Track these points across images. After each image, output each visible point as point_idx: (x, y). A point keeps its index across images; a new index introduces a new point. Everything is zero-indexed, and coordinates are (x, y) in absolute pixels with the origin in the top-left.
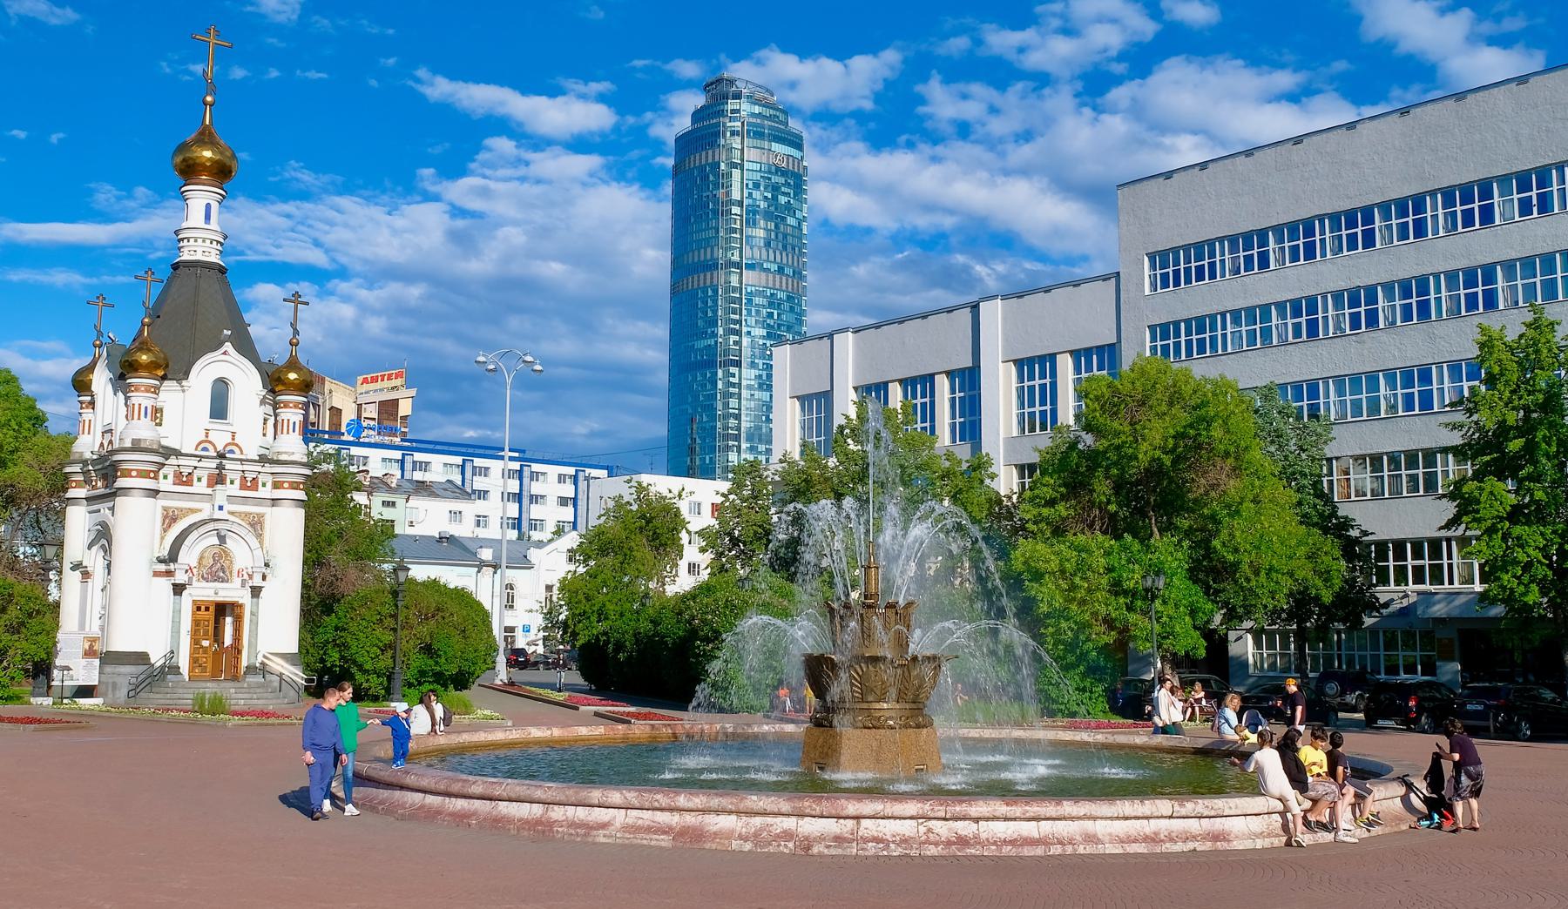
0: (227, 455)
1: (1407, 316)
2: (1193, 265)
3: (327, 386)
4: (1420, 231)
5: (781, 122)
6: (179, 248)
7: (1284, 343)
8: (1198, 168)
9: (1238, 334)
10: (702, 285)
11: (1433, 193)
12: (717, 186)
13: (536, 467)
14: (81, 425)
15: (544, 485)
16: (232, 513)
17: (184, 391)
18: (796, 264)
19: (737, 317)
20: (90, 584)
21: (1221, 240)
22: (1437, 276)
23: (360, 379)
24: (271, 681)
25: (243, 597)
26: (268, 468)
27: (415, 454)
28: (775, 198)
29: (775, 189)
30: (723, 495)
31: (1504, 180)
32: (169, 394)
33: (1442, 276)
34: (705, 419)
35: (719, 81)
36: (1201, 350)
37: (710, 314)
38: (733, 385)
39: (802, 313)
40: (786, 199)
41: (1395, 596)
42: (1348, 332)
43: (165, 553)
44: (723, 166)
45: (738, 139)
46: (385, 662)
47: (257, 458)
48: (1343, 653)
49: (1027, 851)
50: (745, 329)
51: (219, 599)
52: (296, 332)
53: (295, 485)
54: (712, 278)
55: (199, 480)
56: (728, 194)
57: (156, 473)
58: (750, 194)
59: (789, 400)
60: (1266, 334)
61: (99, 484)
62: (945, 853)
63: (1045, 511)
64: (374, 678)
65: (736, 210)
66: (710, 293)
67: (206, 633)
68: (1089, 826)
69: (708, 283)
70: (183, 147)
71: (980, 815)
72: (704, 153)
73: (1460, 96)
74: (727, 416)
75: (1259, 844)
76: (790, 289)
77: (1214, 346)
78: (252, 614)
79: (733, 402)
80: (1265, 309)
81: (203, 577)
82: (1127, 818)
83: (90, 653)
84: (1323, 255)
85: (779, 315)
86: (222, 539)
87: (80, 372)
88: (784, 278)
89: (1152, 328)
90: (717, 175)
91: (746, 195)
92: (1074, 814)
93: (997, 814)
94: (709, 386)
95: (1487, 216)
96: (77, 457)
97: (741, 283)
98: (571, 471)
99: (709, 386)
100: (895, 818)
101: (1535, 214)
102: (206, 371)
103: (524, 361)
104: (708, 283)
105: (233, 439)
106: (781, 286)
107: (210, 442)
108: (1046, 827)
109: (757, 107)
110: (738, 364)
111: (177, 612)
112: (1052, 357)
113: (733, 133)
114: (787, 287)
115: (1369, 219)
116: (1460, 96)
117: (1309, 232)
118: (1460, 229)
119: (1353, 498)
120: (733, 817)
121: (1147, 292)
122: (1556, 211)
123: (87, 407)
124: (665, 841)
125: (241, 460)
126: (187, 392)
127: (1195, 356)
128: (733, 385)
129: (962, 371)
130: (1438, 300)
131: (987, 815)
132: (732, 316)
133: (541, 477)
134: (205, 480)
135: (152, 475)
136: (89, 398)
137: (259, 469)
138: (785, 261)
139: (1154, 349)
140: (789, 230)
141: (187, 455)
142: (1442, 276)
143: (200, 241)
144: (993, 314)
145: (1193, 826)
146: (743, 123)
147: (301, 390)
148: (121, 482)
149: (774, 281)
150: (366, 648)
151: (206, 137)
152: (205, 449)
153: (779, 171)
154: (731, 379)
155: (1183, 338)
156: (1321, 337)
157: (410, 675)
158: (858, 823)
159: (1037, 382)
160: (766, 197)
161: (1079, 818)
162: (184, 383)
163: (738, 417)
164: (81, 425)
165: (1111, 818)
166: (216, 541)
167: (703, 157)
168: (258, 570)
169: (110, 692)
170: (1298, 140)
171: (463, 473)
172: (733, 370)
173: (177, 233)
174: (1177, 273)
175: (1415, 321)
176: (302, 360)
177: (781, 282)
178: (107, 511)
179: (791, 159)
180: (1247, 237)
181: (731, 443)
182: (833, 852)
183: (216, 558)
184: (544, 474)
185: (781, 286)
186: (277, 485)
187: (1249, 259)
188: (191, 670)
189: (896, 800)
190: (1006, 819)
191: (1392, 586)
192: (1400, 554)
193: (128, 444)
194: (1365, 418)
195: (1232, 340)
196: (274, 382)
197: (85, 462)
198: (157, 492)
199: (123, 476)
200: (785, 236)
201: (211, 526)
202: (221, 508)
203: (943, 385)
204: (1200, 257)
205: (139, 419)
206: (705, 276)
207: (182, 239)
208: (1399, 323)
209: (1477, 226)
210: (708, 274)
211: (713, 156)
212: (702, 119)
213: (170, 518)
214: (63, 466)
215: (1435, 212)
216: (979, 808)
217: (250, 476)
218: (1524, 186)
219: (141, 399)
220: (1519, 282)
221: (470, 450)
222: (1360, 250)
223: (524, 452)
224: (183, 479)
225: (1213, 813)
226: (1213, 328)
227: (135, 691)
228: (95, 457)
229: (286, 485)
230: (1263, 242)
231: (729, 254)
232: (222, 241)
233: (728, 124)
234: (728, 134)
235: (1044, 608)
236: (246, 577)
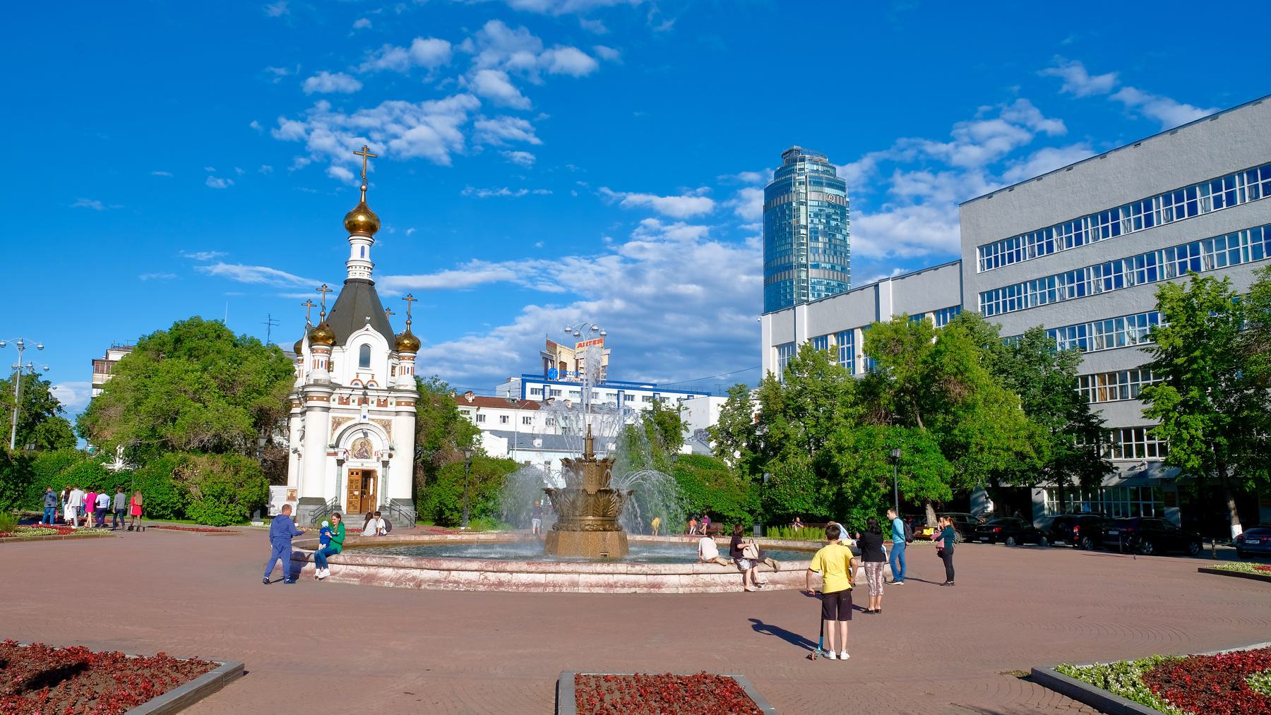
1: (1142, 280)
2: (1006, 252)
3: (558, 349)
4: (1149, 222)
5: (831, 175)
7: (1063, 300)
8: (1008, 190)
9: (1034, 296)
10: (783, 279)
11: (1157, 197)
12: (790, 217)
18: (843, 263)
19: (806, 298)
21: (1023, 235)
22: (1160, 251)
23: (577, 344)
26: (393, 394)
27: (551, 385)
28: (828, 222)
29: (828, 216)
30: (722, 406)
31: (1203, 185)
33: (1163, 251)
35: (791, 151)
36: (1012, 307)
37: (788, 297)
40: (836, 223)
41: (1136, 464)
42: (1103, 291)
43: (334, 443)
44: (794, 204)
45: (804, 187)
48: (1104, 502)
49: (533, 590)
52: (410, 317)
55: (353, 401)
56: (798, 221)
58: (812, 221)
59: (771, 348)
60: (1052, 294)
62: (488, 589)
63: (851, 410)
65: (803, 231)
66: (788, 284)
67: (357, 487)
68: (575, 577)
69: (787, 278)
70: (349, 215)
71: (513, 570)
72: (782, 197)
73: (1173, 131)
75: (681, 591)
76: (839, 280)
77: (1020, 304)
78: (383, 476)
80: (1051, 278)
82: (599, 574)
86: (366, 434)
88: (835, 273)
89: (982, 294)
90: (791, 210)
91: (809, 221)
92: (566, 570)
93: (522, 569)
95: (1193, 210)
97: (807, 276)
100: (466, 570)
101: (1225, 207)
102: (357, 340)
103: (593, 330)
104: (787, 278)
108: (550, 577)
109: (815, 166)
111: (340, 475)
113: (800, 183)
114: (837, 278)
115: (1115, 217)
116: (1173, 131)
117: (1078, 227)
118: (1175, 220)
119: (1108, 400)
120: (391, 569)
122: (1238, 204)
124: (356, 581)
125: (377, 390)
127: (1008, 311)
130: (1161, 267)
131: (516, 570)
132: (803, 298)
134: (356, 402)
135: (325, 399)
137: (387, 395)
138: (836, 262)
140: (838, 242)
142: (1163, 251)
145: (643, 579)
146: (806, 177)
149: (829, 275)
151: (362, 209)
153: (830, 205)
155: (1001, 300)
156: (1086, 295)
158: (450, 573)
161: (570, 573)
162: (344, 347)
165: (589, 573)
167: (782, 199)
170: (1069, 168)
171: (618, 399)
175: (1146, 282)
176: (414, 333)
177: (833, 276)
179: (838, 197)
180: (1039, 232)
182: (432, 588)
183: (363, 445)
184: (668, 398)
186: (398, 404)
187: (1040, 247)
189: (468, 561)
190: (528, 572)
191: (1135, 457)
192: (1139, 436)
193: (312, 382)
194: (1115, 347)
195: (1031, 299)
196: (396, 345)
198: (330, 408)
200: (835, 246)
201: (358, 427)
204: (1010, 247)
206: (785, 274)
208: (1136, 284)
209: (1186, 216)
210: (787, 272)
211: (788, 198)
212: (782, 175)
213: (337, 423)
214: (288, 395)
215: (1159, 208)
216: (512, 566)
217: (382, 399)
218: (1217, 188)
220: (1215, 253)
221: (623, 385)
222: (1111, 237)
224: (345, 401)
225: (653, 572)
230: (1050, 236)
231: (800, 259)
233: (797, 178)
234: (797, 184)
235: (843, 471)
236: (380, 456)
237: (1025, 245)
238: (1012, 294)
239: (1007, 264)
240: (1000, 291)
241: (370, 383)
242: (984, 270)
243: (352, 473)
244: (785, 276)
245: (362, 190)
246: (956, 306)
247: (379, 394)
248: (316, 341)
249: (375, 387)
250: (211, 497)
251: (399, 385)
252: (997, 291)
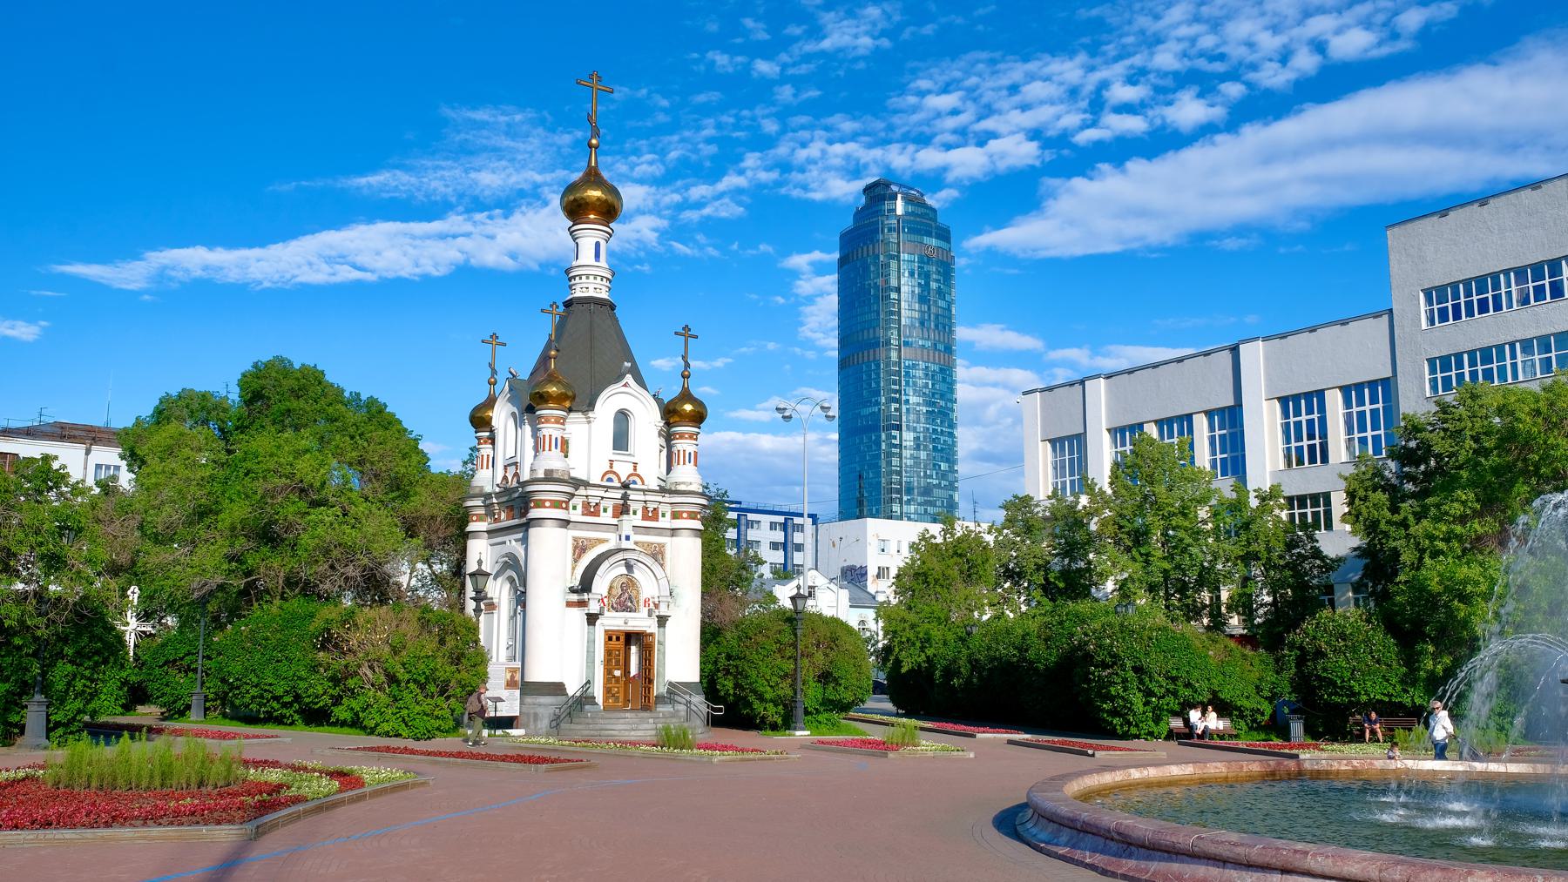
0: (631, 486)
6: (570, 287)
13: (751, 516)
14: (480, 460)
15: (758, 531)
16: (636, 543)
17: (589, 422)
20: (496, 616)
24: (678, 711)
25: (649, 626)
26: (668, 499)
32: (575, 427)
34: (871, 475)
37: (873, 385)
38: (895, 446)
39: (953, 383)
43: (576, 583)
44: (882, 258)
45: (895, 235)
46: (785, 690)
47: (658, 488)
50: (904, 398)
51: (628, 628)
52: (687, 365)
53: (693, 515)
54: (874, 354)
55: (605, 510)
56: (887, 282)
57: (567, 503)
59: (1040, 444)
61: (503, 516)
64: (770, 706)
67: (618, 662)
69: (871, 359)
70: (571, 188)
74: (892, 473)
79: (895, 461)
81: (612, 606)
83: (511, 684)
84: (1510, 306)
85: (933, 385)
87: (477, 409)
90: (876, 264)
91: (902, 282)
94: (874, 447)
96: (477, 491)
97: (900, 357)
98: (781, 519)
99: (874, 447)
102: (610, 402)
104: (871, 359)
105: (635, 470)
106: (934, 360)
107: (615, 473)
110: (899, 428)
111: (591, 642)
112: (1189, 417)
113: (890, 230)
123: (485, 443)
125: (644, 491)
126: (593, 424)
128: (895, 446)
129: (1221, 411)
132: (893, 387)
133: (755, 525)
134: (610, 511)
135: (564, 505)
136: (488, 434)
137: (659, 499)
141: (594, 486)
143: (591, 277)
144: (1254, 356)
147: (694, 421)
148: (535, 513)
150: (766, 677)
152: (610, 480)
154: (894, 441)
157: (810, 704)
159: (1304, 418)
160: (919, 284)
162: (590, 414)
163: (899, 473)
164: (480, 460)
166: (623, 570)
168: (664, 599)
169: (532, 723)
172: (895, 433)
173: (567, 271)
177: (934, 357)
178: (513, 543)
181: (894, 496)
185: (934, 360)
186: (675, 515)
188: (606, 700)
193: (541, 475)
197: (488, 496)
199: (537, 506)
201: (620, 556)
202: (628, 538)
203: (1201, 424)
205: (550, 450)
206: (868, 352)
207: (574, 277)
210: (871, 351)
213: (580, 549)
214: (464, 499)
219: (549, 430)
223: (740, 503)
224: (591, 510)
226: (1501, 357)
227: (556, 722)
228: (497, 490)
232: (610, 277)
234: (886, 230)
236: (652, 606)
241: (631, 479)
243: (610, 636)
244: (868, 356)
245: (590, 146)
246: (1383, 380)
247: (648, 498)
248: (546, 401)
249: (639, 486)
250: (411, 685)
251: (679, 484)
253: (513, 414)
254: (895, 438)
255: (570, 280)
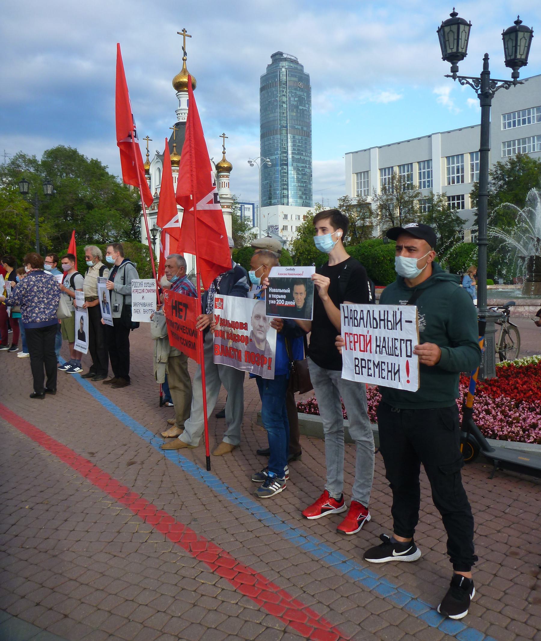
121: (502, 129)
139: (504, 151)
172: (285, 167)
174: (514, 122)
207: (179, 114)
229: (225, 207)
237: (534, 114)
238: (524, 143)
239: (517, 126)
240: (516, 141)
242: (505, 128)
251: (223, 195)
252: (514, 141)
253: (159, 169)
254: (285, 169)
255: (177, 114)
